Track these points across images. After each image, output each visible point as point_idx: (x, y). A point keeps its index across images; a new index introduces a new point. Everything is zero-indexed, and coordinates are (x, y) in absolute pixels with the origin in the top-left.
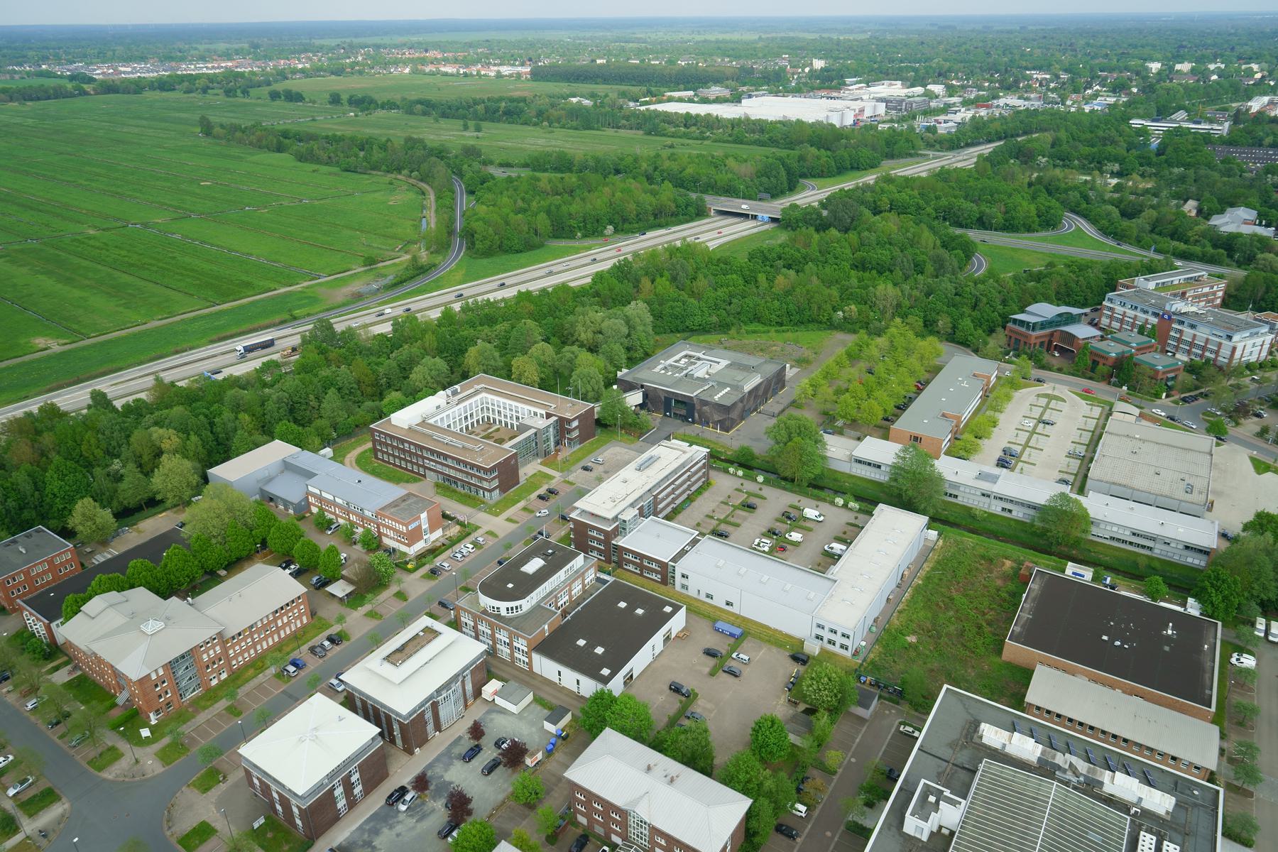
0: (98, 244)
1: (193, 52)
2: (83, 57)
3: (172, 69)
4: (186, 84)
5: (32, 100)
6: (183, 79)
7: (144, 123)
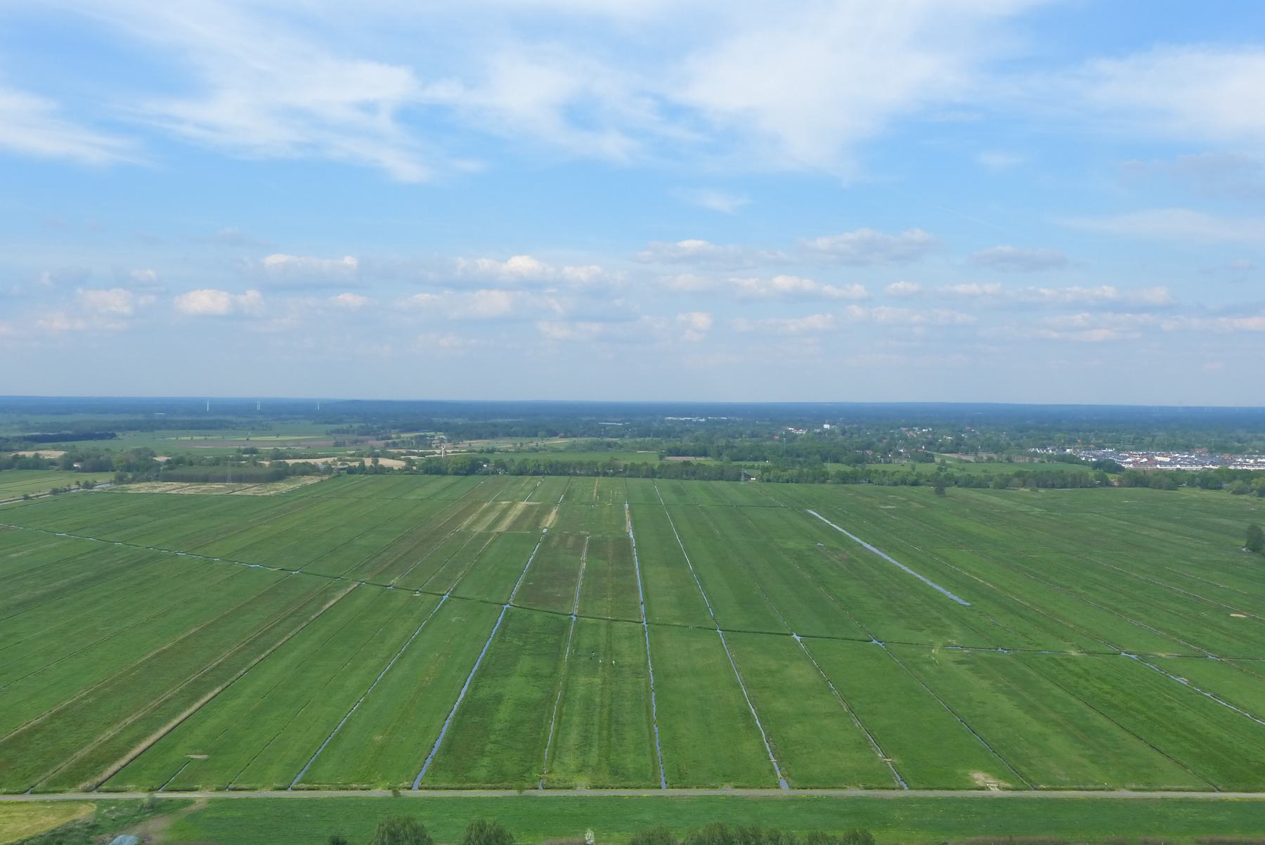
0: (1077, 669)
1: (1255, 443)
2: (1116, 442)
3: (1223, 462)
4: (1238, 483)
5: (1045, 486)
6: (1235, 475)
7: (1172, 526)
